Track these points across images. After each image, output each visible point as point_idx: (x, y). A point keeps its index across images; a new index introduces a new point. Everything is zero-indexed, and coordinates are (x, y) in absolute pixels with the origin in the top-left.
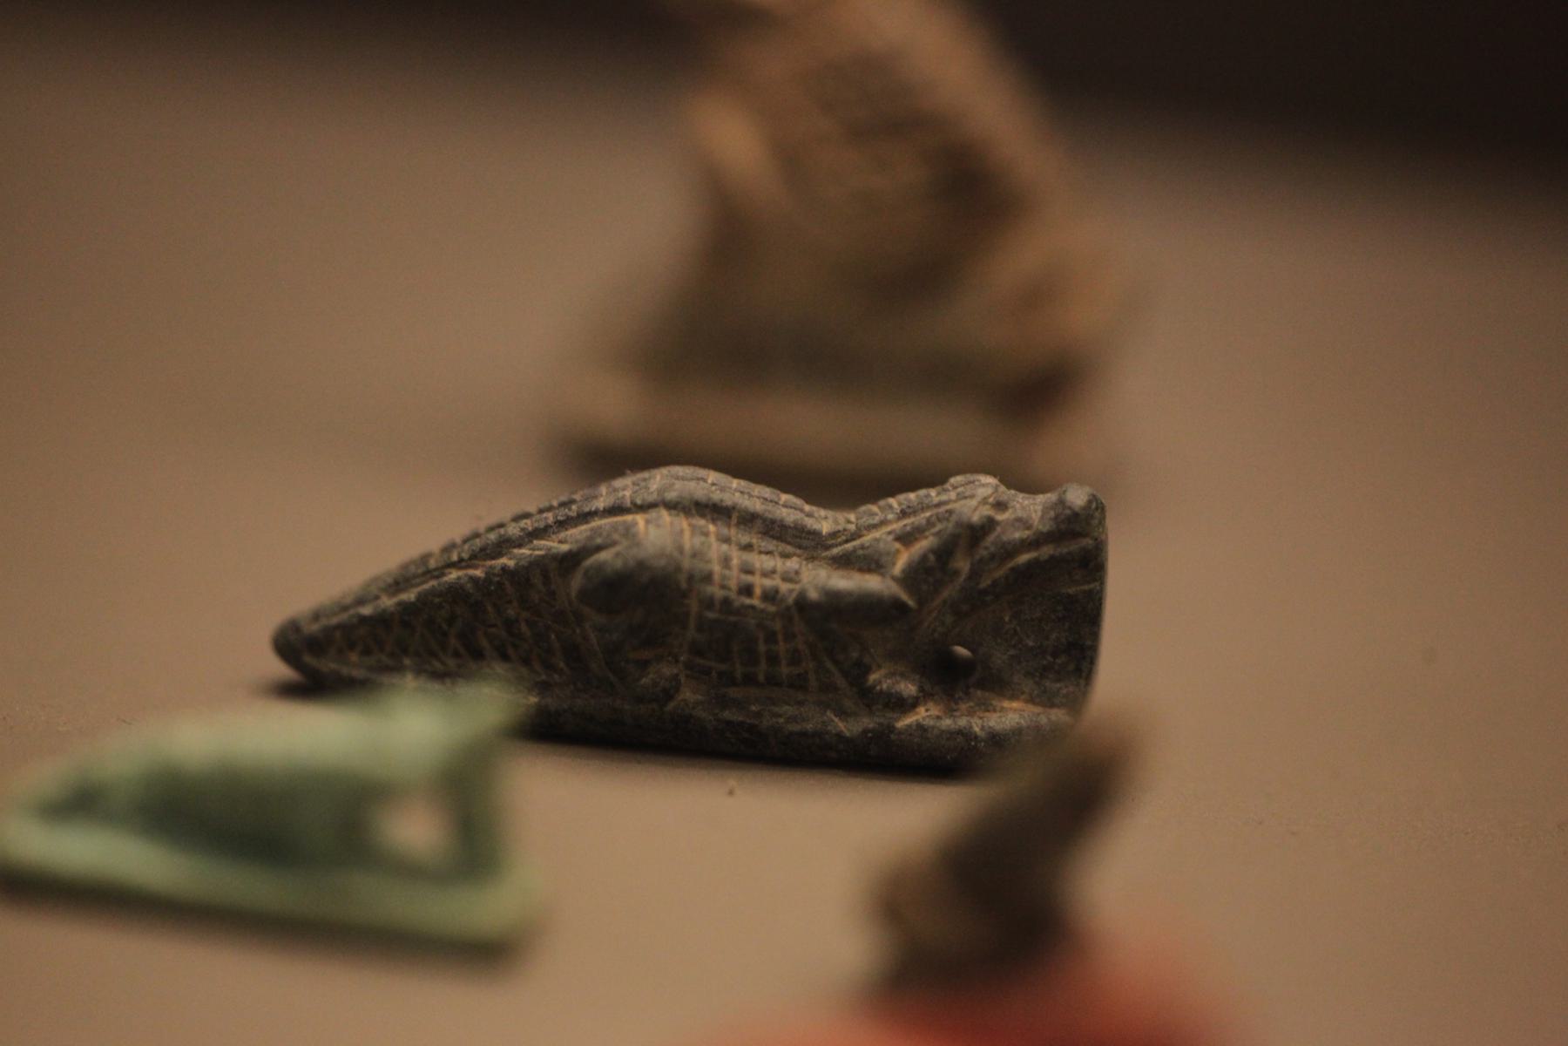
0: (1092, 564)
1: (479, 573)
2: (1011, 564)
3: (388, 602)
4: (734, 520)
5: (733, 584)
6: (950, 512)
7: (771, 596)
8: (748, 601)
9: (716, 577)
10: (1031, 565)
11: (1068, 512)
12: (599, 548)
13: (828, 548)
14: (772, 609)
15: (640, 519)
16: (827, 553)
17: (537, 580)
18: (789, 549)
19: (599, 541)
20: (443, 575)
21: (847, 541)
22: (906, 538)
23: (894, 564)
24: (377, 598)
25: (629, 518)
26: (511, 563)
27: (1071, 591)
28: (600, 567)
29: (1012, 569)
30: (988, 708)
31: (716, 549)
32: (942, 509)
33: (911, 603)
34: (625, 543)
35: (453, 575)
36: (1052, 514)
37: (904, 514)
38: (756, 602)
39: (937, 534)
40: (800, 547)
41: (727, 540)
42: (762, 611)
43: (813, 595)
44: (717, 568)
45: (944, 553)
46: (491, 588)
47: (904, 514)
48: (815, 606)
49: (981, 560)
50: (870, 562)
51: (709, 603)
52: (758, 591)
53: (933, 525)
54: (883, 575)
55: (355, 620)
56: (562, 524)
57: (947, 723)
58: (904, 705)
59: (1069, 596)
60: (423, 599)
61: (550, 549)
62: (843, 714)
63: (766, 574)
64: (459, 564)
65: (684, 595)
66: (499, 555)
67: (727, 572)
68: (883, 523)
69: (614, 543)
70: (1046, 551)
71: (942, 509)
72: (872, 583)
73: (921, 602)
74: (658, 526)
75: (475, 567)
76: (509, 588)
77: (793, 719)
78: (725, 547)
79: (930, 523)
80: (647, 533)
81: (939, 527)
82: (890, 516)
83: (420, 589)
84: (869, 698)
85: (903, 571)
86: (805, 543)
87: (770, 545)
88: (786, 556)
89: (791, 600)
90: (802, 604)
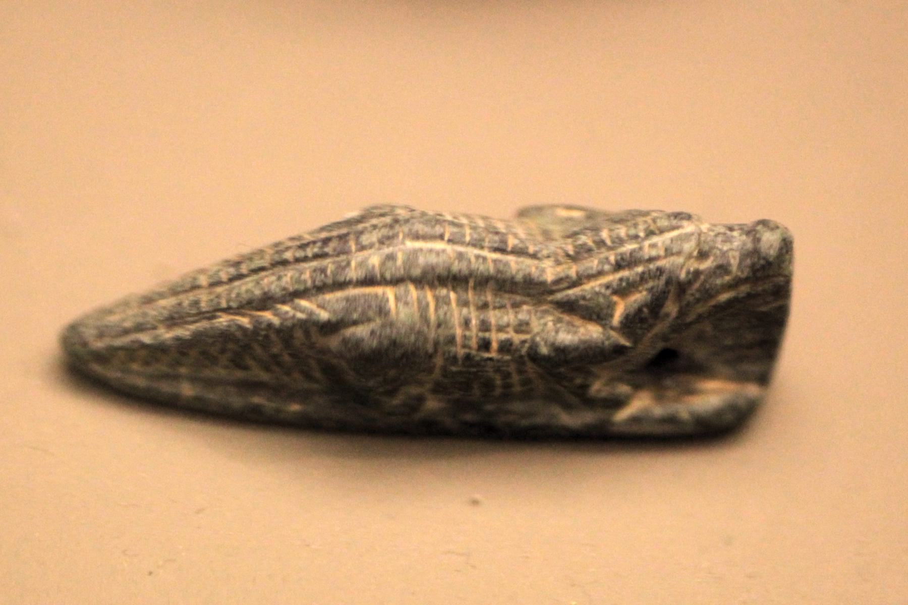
0: (782, 291)
1: (245, 321)
2: (713, 302)
3: (167, 335)
4: (471, 283)
5: (474, 343)
6: (660, 271)
7: (506, 347)
8: (486, 355)
9: (458, 339)
10: (730, 303)
11: (762, 262)
12: (355, 323)
13: (552, 292)
14: (507, 357)
15: (390, 293)
16: (550, 298)
17: (299, 334)
18: (518, 298)
19: (355, 316)
20: (214, 317)
21: (569, 288)
22: (623, 290)
23: (612, 316)
24: (155, 328)
25: (379, 290)
26: (276, 321)
27: (764, 309)
28: (358, 342)
29: (715, 306)
30: (691, 392)
31: (456, 314)
32: (652, 266)
33: (628, 344)
34: (379, 321)
35: (223, 320)
36: (748, 262)
37: (618, 266)
38: (493, 354)
39: (650, 290)
40: (529, 295)
41: (466, 304)
42: (498, 361)
43: (544, 350)
44: (459, 332)
45: (655, 306)
46: (261, 336)
47: (618, 266)
48: (547, 359)
49: (688, 305)
50: (595, 313)
51: (454, 359)
52: (495, 345)
53: (647, 282)
54: (604, 326)
55: (137, 345)
56: (321, 288)
57: (658, 411)
58: (618, 403)
59: (763, 313)
60: (198, 339)
61: (311, 313)
62: (568, 407)
63: (501, 329)
64: (228, 310)
65: (431, 357)
66: (263, 308)
67: (468, 333)
68: (600, 273)
69: (369, 320)
70: (744, 289)
71: (652, 266)
72: (592, 332)
73: (636, 342)
74: (406, 303)
75: (243, 315)
76: (273, 336)
77: (523, 416)
78: (465, 311)
79: (643, 278)
80: (397, 313)
81: (651, 284)
82: (607, 267)
83: (192, 327)
84: (590, 403)
85: (621, 322)
86: (532, 292)
87: (506, 299)
88: (516, 306)
89: (524, 351)
90: (534, 355)
